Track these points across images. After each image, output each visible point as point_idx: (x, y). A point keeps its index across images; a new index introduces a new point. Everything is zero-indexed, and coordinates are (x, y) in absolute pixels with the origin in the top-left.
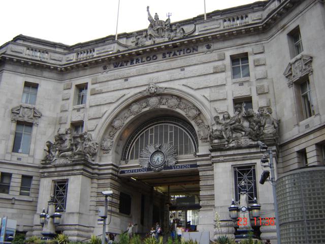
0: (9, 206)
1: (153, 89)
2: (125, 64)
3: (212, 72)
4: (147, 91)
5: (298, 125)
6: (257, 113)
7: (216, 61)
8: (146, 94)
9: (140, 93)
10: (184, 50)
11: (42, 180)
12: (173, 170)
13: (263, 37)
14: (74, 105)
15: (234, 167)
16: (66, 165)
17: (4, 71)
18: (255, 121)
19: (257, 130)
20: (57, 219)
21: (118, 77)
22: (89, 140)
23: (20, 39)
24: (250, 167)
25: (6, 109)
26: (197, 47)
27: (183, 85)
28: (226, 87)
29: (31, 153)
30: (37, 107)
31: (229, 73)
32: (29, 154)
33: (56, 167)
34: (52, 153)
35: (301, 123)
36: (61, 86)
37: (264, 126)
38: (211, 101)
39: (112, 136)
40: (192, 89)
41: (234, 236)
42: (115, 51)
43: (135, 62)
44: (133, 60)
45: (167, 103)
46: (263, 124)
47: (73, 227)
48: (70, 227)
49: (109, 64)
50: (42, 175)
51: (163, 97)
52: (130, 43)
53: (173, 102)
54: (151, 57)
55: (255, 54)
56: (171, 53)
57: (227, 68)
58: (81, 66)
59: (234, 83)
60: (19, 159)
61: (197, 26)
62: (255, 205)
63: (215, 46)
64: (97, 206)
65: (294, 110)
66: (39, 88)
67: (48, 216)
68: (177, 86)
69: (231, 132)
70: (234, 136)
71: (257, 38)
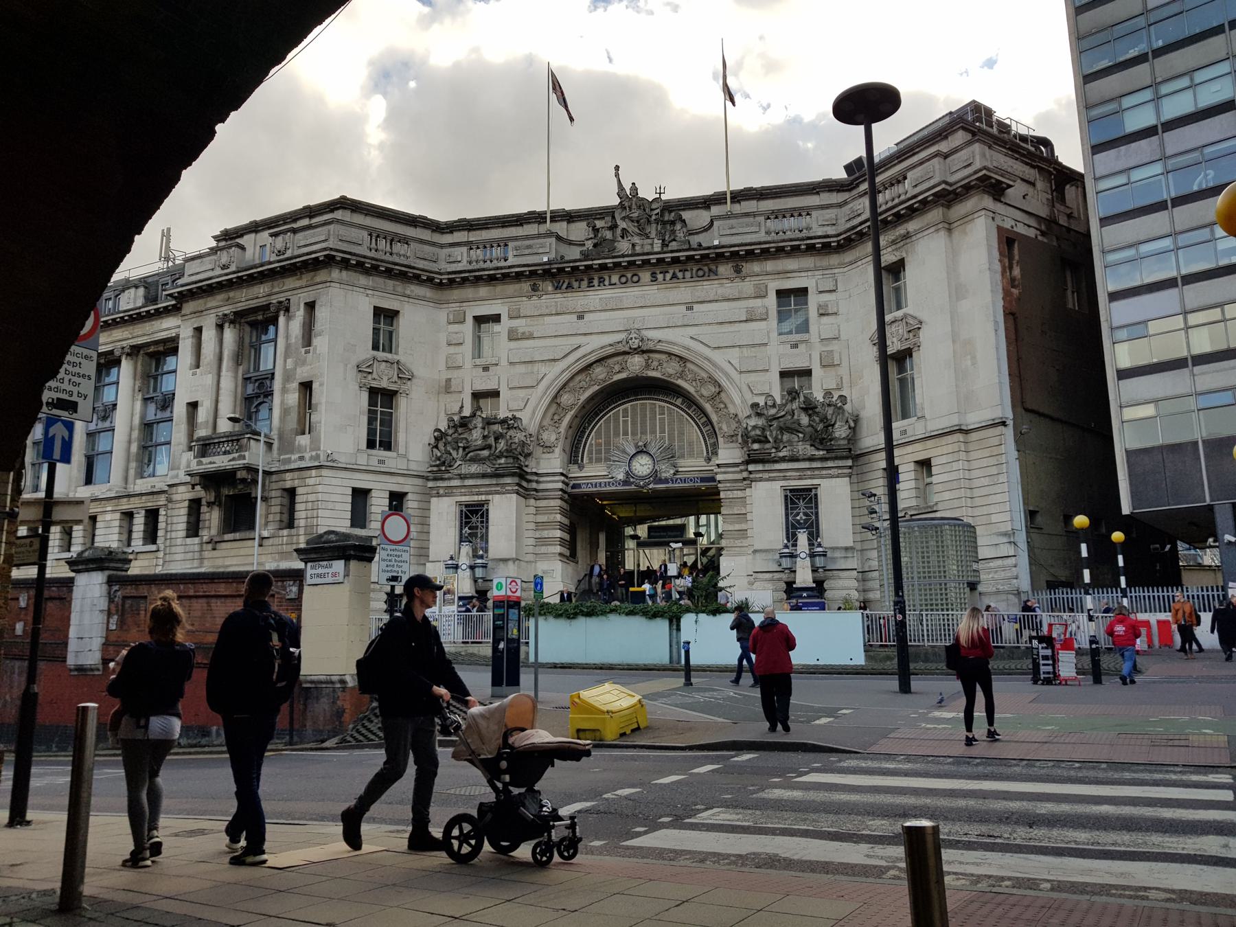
1: (637, 341)
2: (576, 284)
4: (624, 343)
8: (621, 348)
9: (611, 345)
11: (434, 500)
12: (670, 485)
13: (834, 259)
16: (484, 476)
17: (332, 284)
20: (479, 573)
23: (345, 208)
24: (810, 490)
29: (402, 450)
30: (401, 357)
33: (462, 477)
36: (442, 315)
37: (833, 425)
41: (785, 596)
42: (553, 256)
43: (596, 282)
54: (629, 276)
55: (821, 292)
60: (381, 462)
62: (820, 549)
68: (678, 339)
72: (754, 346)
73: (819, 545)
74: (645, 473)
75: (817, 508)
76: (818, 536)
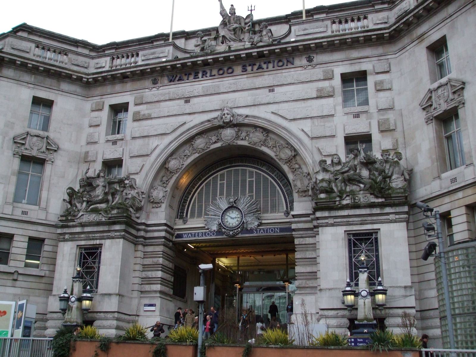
0: (10, 283)
1: (229, 116)
2: (185, 78)
3: (315, 96)
4: (219, 119)
5: (439, 177)
6: (380, 157)
7: (320, 80)
8: (217, 123)
9: (209, 121)
10: (274, 62)
11: (61, 244)
12: (255, 235)
14: (107, 134)
15: (348, 233)
16: (99, 224)
18: (377, 170)
19: (381, 182)
20: (86, 303)
21: (176, 96)
22: (132, 187)
24: (371, 234)
25: (5, 137)
26: (293, 59)
27: (272, 113)
28: (334, 117)
29: (43, 204)
30: (52, 134)
31: (339, 99)
32: (39, 205)
33: (82, 225)
34: (77, 204)
35: (444, 175)
36: (88, 105)
37: (390, 177)
38: (312, 138)
39: (164, 184)
40: (286, 119)
42: (170, 58)
43: (200, 75)
44: (199, 73)
45: (247, 138)
46: (390, 174)
47: (110, 316)
48: (106, 315)
49: (162, 76)
50: (62, 237)
51: (242, 128)
52: (191, 45)
53: (256, 137)
54: (225, 69)
55: (378, 73)
56: (255, 65)
57: (336, 91)
58: (118, 77)
59: (347, 114)
60: (24, 213)
61: (293, 28)
62: (380, 288)
63: (318, 58)
64: (142, 284)
65: (434, 156)
66: (55, 108)
67: (73, 299)
69: (343, 184)
70: (348, 189)
71: (380, 50)
72: (323, 117)
73: (380, 284)
74: (234, 225)
75: (377, 250)
76: (379, 275)
